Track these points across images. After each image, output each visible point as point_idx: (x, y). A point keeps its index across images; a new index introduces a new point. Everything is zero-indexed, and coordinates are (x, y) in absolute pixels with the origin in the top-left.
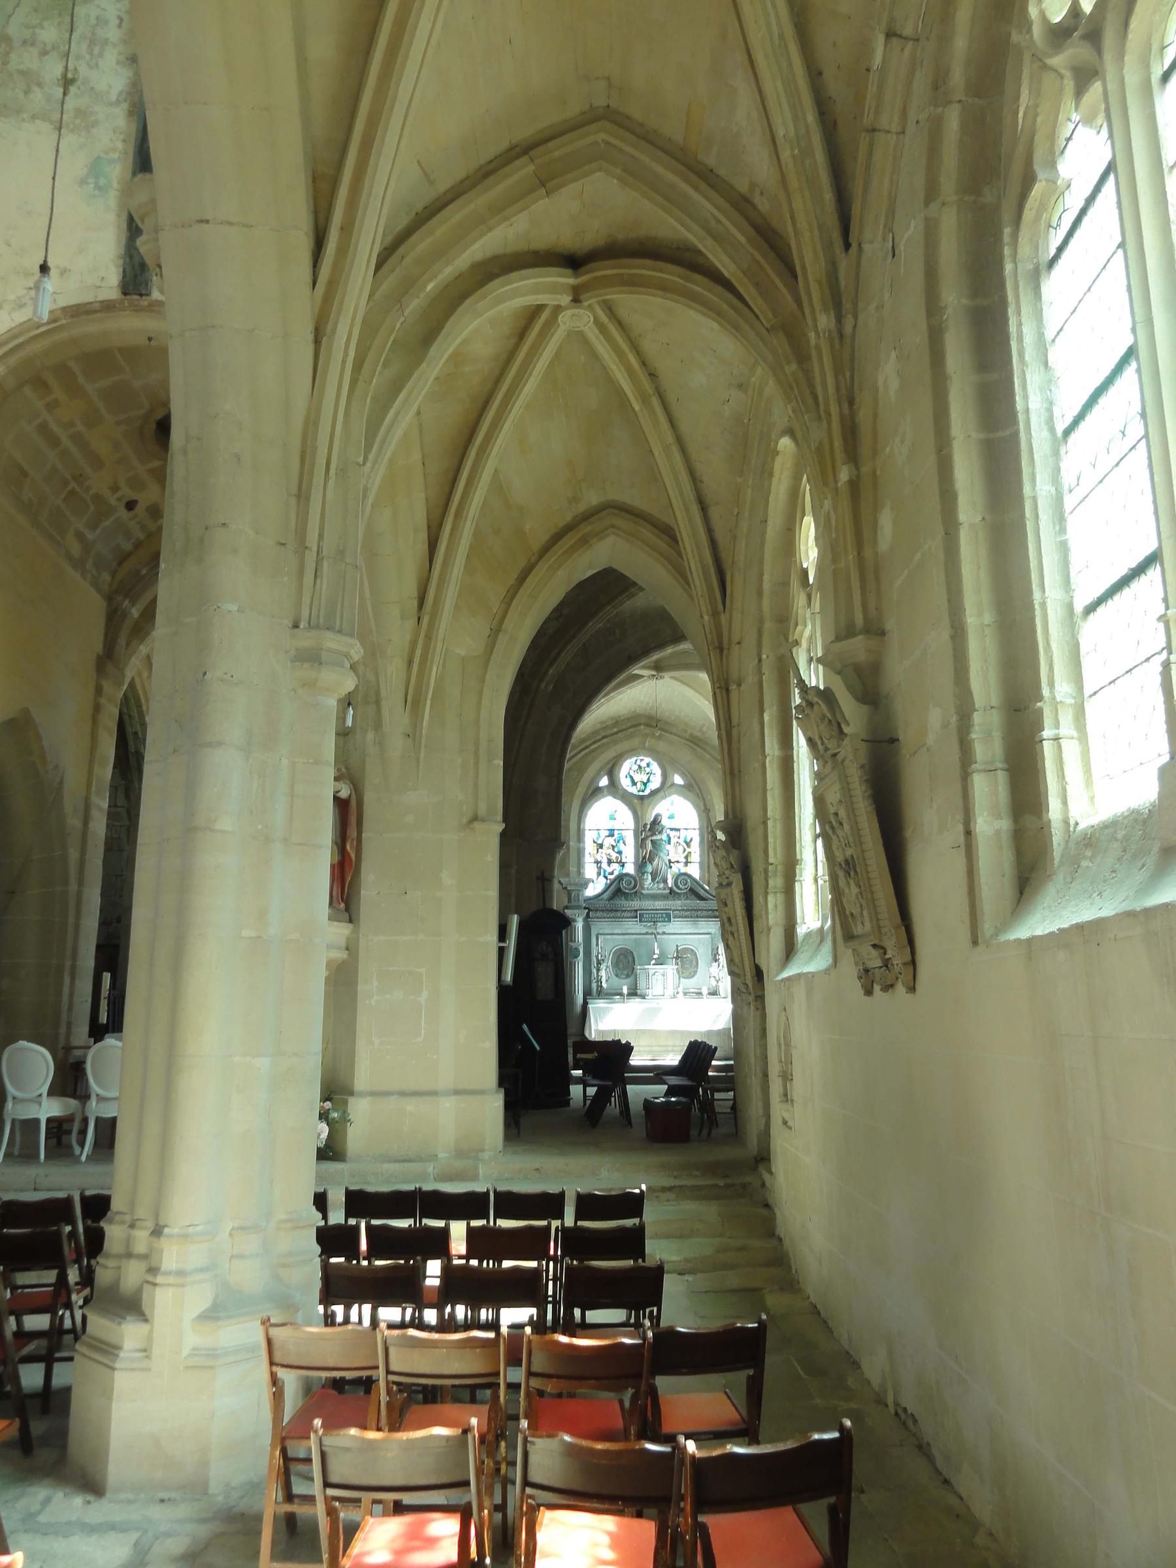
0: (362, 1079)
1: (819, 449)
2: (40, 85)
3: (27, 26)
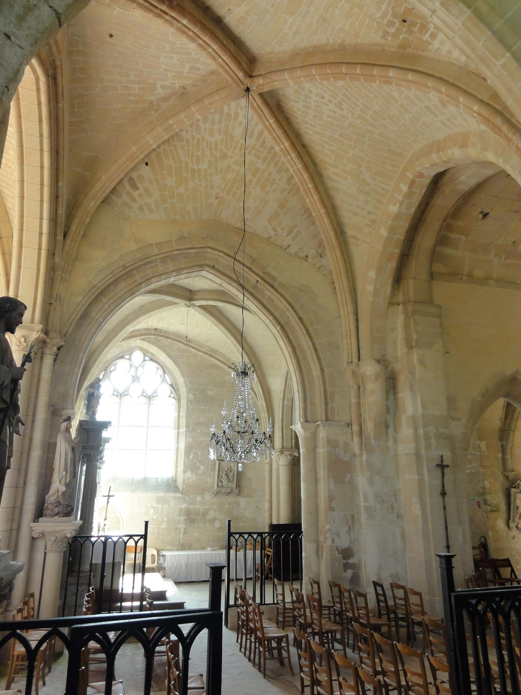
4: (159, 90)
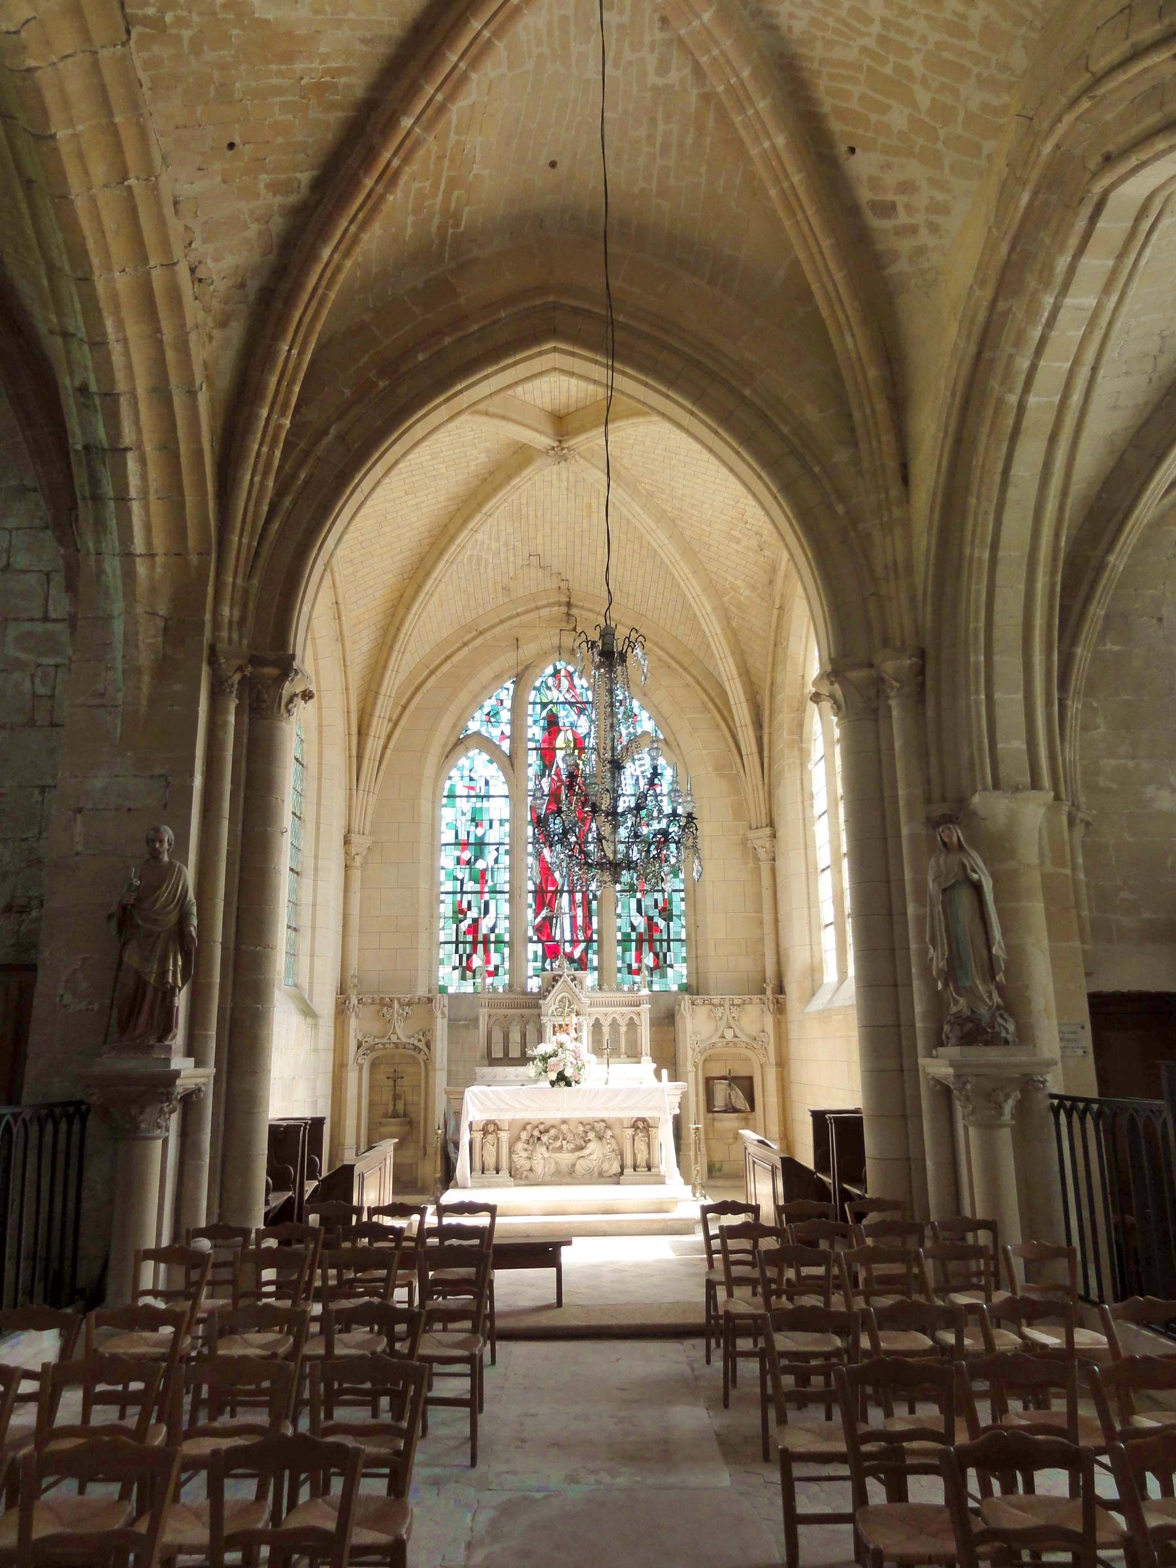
4: (673, 77)
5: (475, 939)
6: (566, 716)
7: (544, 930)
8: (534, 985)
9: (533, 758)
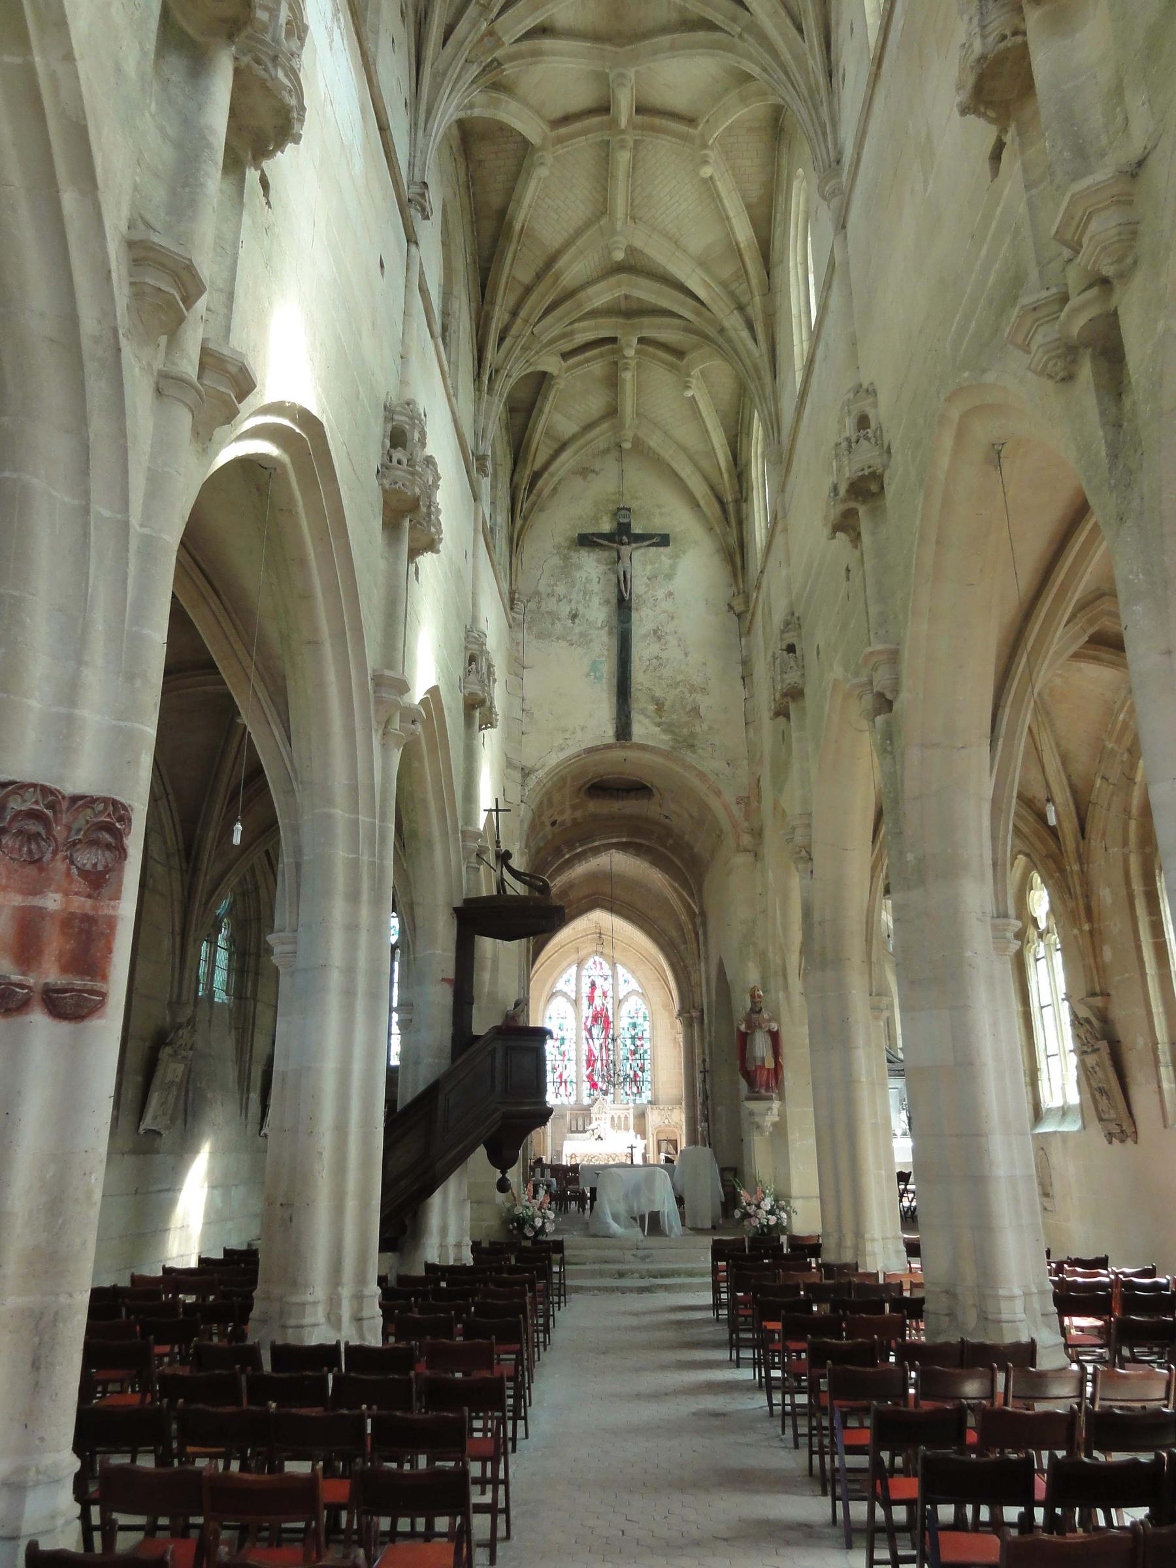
0: (795, 1190)
1: (1072, 912)
2: (559, 619)
3: (548, 585)
5: (562, 1082)
6: (599, 982)
7: (590, 1077)
8: (586, 1101)
9: (585, 1002)
